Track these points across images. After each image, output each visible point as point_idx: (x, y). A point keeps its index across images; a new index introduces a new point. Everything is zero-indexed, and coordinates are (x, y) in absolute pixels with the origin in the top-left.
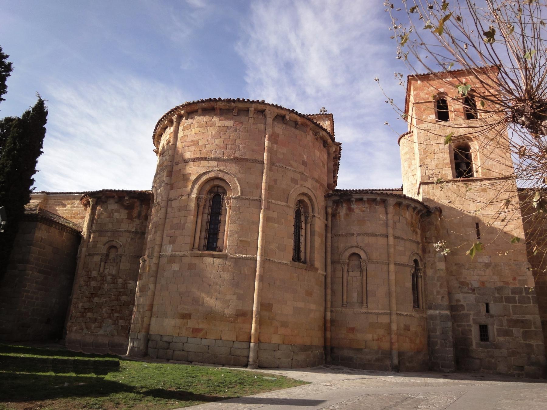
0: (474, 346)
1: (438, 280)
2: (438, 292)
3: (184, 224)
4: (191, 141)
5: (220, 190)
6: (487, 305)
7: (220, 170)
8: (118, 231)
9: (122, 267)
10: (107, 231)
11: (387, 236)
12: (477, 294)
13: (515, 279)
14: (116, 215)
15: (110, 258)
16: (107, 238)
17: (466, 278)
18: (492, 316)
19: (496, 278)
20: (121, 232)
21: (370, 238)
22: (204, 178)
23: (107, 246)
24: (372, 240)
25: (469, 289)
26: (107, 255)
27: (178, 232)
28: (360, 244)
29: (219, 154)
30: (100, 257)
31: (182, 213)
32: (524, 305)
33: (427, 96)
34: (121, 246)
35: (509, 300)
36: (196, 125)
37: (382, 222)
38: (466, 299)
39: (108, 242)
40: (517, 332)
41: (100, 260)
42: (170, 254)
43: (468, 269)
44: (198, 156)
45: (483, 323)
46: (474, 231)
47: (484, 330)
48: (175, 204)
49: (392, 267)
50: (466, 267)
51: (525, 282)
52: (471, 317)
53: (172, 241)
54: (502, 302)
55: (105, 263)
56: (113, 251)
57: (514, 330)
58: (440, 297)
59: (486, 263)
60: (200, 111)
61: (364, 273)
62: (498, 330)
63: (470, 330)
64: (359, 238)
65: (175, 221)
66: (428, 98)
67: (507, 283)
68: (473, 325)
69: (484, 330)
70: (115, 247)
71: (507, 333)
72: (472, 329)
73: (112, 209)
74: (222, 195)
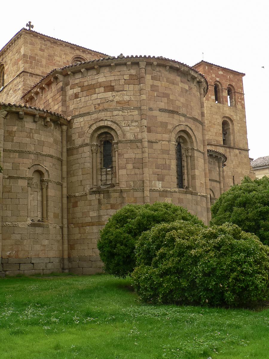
3: (170, 166)
4: (163, 93)
7: (187, 126)
10: (29, 153)
11: (220, 183)
14: (36, 136)
16: (31, 161)
22: (178, 129)
23: (33, 170)
27: (165, 172)
31: (166, 156)
33: (211, 81)
34: (47, 171)
42: (162, 189)
44: (171, 109)
48: (155, 146)
53: (161, 178)
60: (168, 68)
65: (160, 162)
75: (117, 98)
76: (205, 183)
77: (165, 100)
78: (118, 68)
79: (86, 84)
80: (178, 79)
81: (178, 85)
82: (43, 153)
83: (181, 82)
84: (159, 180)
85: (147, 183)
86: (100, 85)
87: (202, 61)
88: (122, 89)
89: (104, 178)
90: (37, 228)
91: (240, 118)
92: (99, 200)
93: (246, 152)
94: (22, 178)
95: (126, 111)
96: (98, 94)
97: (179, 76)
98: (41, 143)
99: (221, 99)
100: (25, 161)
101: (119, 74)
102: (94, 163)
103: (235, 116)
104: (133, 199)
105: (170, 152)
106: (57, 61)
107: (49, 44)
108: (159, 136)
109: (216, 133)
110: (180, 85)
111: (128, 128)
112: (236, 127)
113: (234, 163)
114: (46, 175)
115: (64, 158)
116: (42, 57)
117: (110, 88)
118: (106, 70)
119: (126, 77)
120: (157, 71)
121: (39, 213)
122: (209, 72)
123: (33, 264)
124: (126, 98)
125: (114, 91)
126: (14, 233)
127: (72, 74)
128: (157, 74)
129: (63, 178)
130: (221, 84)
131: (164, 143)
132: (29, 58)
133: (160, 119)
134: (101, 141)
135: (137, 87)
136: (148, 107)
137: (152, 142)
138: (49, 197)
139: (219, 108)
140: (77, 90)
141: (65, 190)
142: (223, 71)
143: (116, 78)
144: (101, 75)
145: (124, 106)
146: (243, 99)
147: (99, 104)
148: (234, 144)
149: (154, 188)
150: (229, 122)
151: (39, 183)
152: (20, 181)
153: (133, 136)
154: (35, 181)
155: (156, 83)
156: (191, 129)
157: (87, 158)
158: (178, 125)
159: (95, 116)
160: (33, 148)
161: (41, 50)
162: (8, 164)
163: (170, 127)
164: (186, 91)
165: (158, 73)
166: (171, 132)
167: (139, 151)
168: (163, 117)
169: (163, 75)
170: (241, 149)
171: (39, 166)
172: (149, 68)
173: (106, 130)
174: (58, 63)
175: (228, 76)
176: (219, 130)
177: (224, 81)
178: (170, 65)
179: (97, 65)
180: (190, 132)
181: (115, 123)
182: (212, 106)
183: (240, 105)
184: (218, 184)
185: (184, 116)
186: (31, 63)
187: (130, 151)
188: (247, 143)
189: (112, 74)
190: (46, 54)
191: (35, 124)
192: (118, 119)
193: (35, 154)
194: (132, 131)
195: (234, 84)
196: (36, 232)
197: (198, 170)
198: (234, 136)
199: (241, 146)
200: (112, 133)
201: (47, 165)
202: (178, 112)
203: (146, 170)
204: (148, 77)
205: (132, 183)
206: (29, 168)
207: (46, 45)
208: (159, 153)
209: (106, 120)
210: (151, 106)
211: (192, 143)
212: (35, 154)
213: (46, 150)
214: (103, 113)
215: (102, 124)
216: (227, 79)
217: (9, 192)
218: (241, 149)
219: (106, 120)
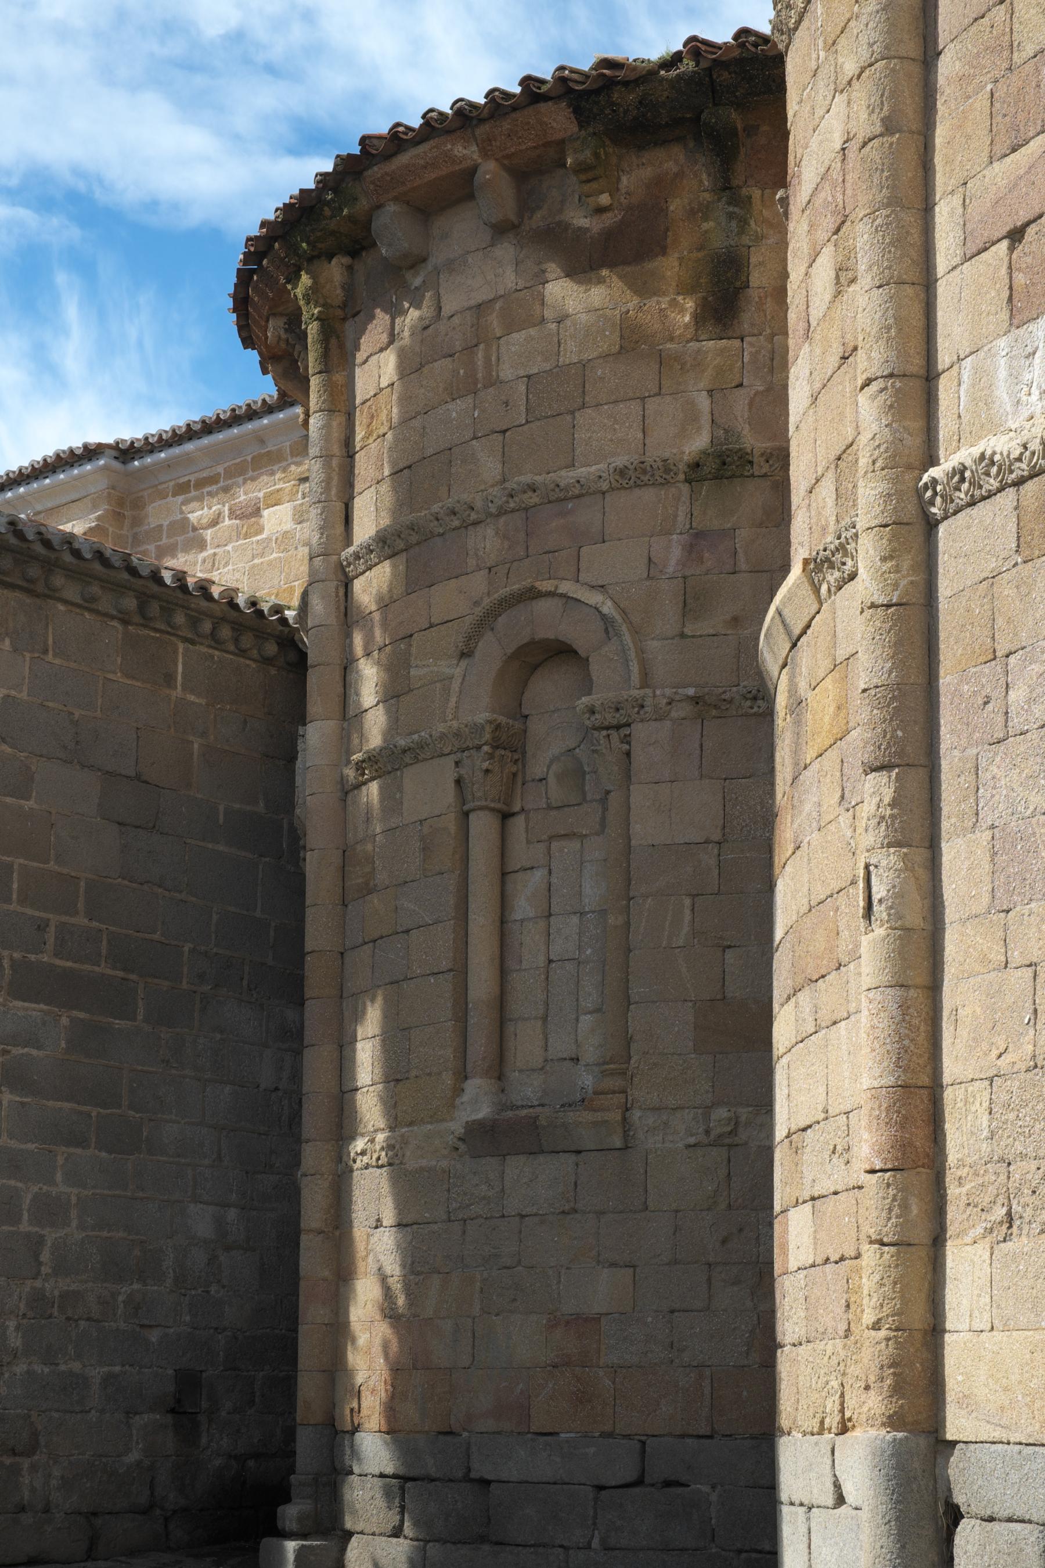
8: (561, 498)
9: (646, 830)
15: (537, 768)
20: (583, 492)
23: (492, 652)
26: (509, 743)
30: (445, 771)
39: (487, 620)
41: (449, 795)
55: (506, 816)
56: (548, 688)
70: (561, 652)
73: (481, 309)
90: (517, 1167)
121: (586, 1021)
123: (485, 1483)
171: (542, 606)
193: (502, 512)
206: (465, 654)
212: (502, 512)
217: (368, 889)
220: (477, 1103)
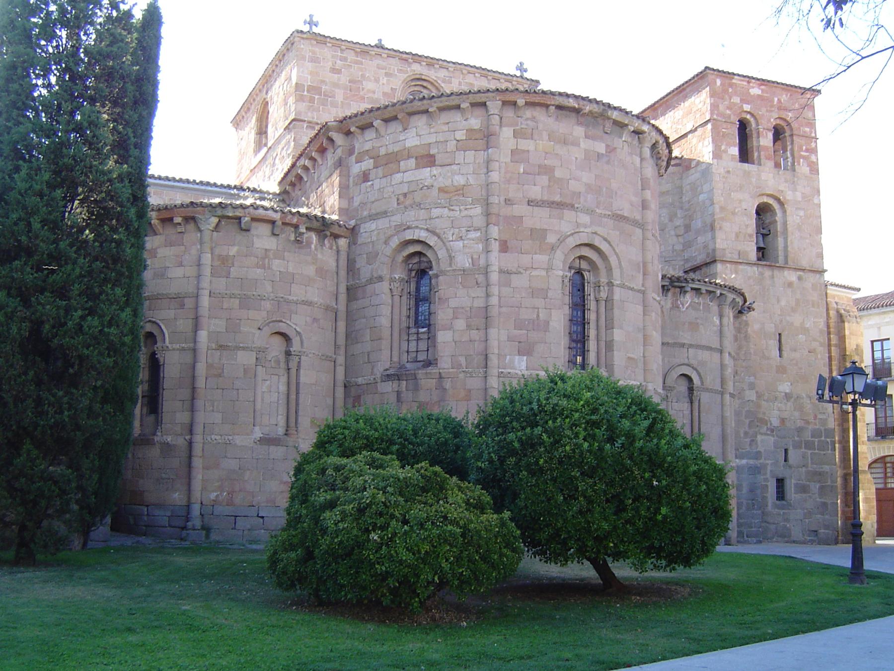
0: (770, 508)
1: (746, 417)
2: (746, 433)
4: (539, 166)
5: (584, 265)
6: (786, 451)
7: (595, 233)
12: (776, 438)
13: (815, 417)
14: (277, 265)
16: (264, 314)
17: (764, 413)
18: (790, 467)
19: (797, 414)
21: (705, 352)
22: (572, 242)
23: (267, 331)
24: (704, 355)
25: (768, 429)
28: (693, 362)
29: (589, 200)
31: (539, 302)
32: (822, 452)
33: (728, 112)
34: (298, 333)
35: (809, 445)
36: (545, 137)
37: (715, 328)
38: (765, 442)
40: (815, 487)
43: (767, 401)
44: (557, 198)
45: (780, 476)
46: (774, 344)
47: (780, 482)
48: (516, 281)
49: (727, 397)
50: (766, 398)
51: (824, 422)
52: (769, 468)
53: (526, 350)
54: (801, 448)
57: (812, 485)
58: (748, 440)
59: (786, 394)
60: (552, 108)
61: (696, 405)
62: (796, 485)
63: (767, 486)
64: (692, 351)
65: (526, 315)
66: (729, 117)
67: (808, 422)
68: (770, 479)
69: (780, 482)
71: (803, 489)
72: (769, 484)
74: (586, 274)
75: (442, 182)
76: (644, 357)
77: (544, 180)
78: (445, 117)
79: (383, 151)
80: (579, 131)
81: (579, 145)
82: (291, 298)
83: (587, 137)
84: (520, 353)
85: (494, 360)
86: (408, 154)
87: (706, 68)
88: (449, 161)
89: (413, 346)
90: (272, 448)
91: (804, 196)
92: (399, 393)
93: (818, 276)
94: (244, 349)
95: (457, 208)
96: (404, 172)
97: (579, 124)
98: (289, 279)
99: (756, 154)
100: (252, 314)
101: (445, 128)
102: (396, 317)
103: (790, 193)
104: (463, 394)
105: (550, 294)
106: (369, 91)
107: (351, 56)
108: (526, 259)
109: (737, 236)
110: (582, 145)
111: (461, 244)
112: (791, 219)
113: (783, 303)
114: (296, 341)
115: (342, 307)
116: (336, 85)
117: (428, 160)
118: (420, 122)
119: (461, 135)
120: (527, 119)
121: (280, 417)
122: (725, 91)
123: (263, 517)
124: (460, 180)
125: (434, 166)
126: (226, 457)
127: (358, 131)
128: (527, 125)
129: (336, 346)
130: (755, 118)
131: (535, 273)
132: (308, 91)
133: (528, 223)
134: (411, 270)
135: (481, 156)
136: (502, 199)
137: (509, 273)
138: (301, 386)
139: (747, 174)
140: (368, 164)
141: (341, 371)
142: (763, 87)
143: (441, 138)
144: (412, 132)
145: (453, 194)
146: (814, 151)
147: (405, 195)
148: (786, 257)
149: (509, 371)
150: (776, 206)
151: (282, 358)
152: (240, 353)
153: (470, 260)
154: (273, 354)
155: (525, 144)
156: (605, 239)
157: (386, 306)
158: (572, 234)
159: (397, 219)
160: (269, 289)
161: (334, 71)
162: (217, 321)
163: (551, 239)
164: (599, 156)
165: (529, 122)
166: (553, 248)
167: (480, 292)
168: (539, 218)
169: (541, 126)
170: (803, 270)
171: (281, 324)
172: (509, 113)
173: (417, 248)
174: (370, 95)
175: (776, 99)
176: (747, 226)
177: (764, 110)
178: (557, 103)
179: (402, 111)
180: (604, 247)
181: (434, 233)
182: (728, 172)
183: (805, 164)
184: (716, 356)
185: (590, 212)
186: (312, 100)
187: (461, 292)
188: (820, 256)
189: (432, 130)
190: (344, 79)
191: (274, 240)
192: (440, 225)
194: (467, 250)
195: (790, 116)
196: (272, 457)
197: (621, 328)
198: (786, 239)
199: (804, 263)
200: (429, 254)
201: (297, 322)
202: (573, 206)
203: (493, 332)
204: (507, 133)
205: (462, 360)
207: (344, 59)
208: (524, 295)
209: (417, 227)
210: (511, 195)
211: (609, 269)
213: (298, 292)
214: (412, 213)
215: (409, 235)
216: (772, 106)
217: (220, 376)
218: (803, 270)
219: (417, 227)
220: (258, 434)
